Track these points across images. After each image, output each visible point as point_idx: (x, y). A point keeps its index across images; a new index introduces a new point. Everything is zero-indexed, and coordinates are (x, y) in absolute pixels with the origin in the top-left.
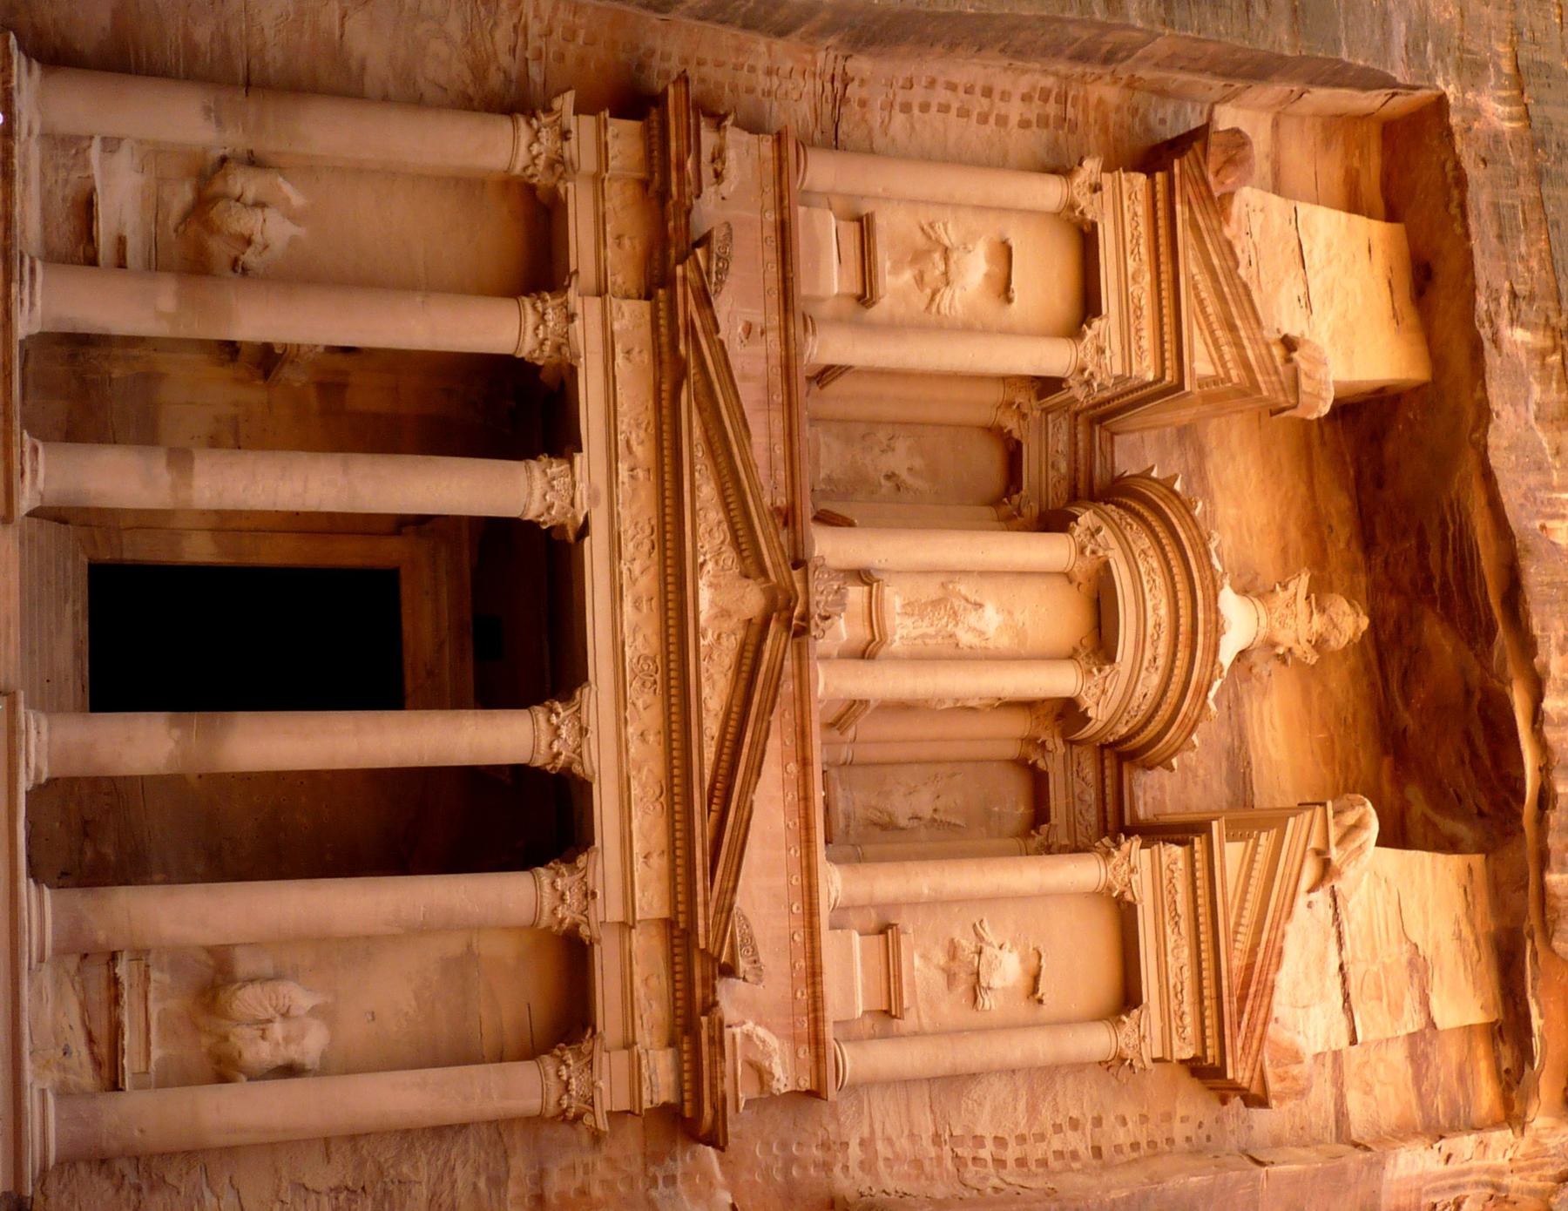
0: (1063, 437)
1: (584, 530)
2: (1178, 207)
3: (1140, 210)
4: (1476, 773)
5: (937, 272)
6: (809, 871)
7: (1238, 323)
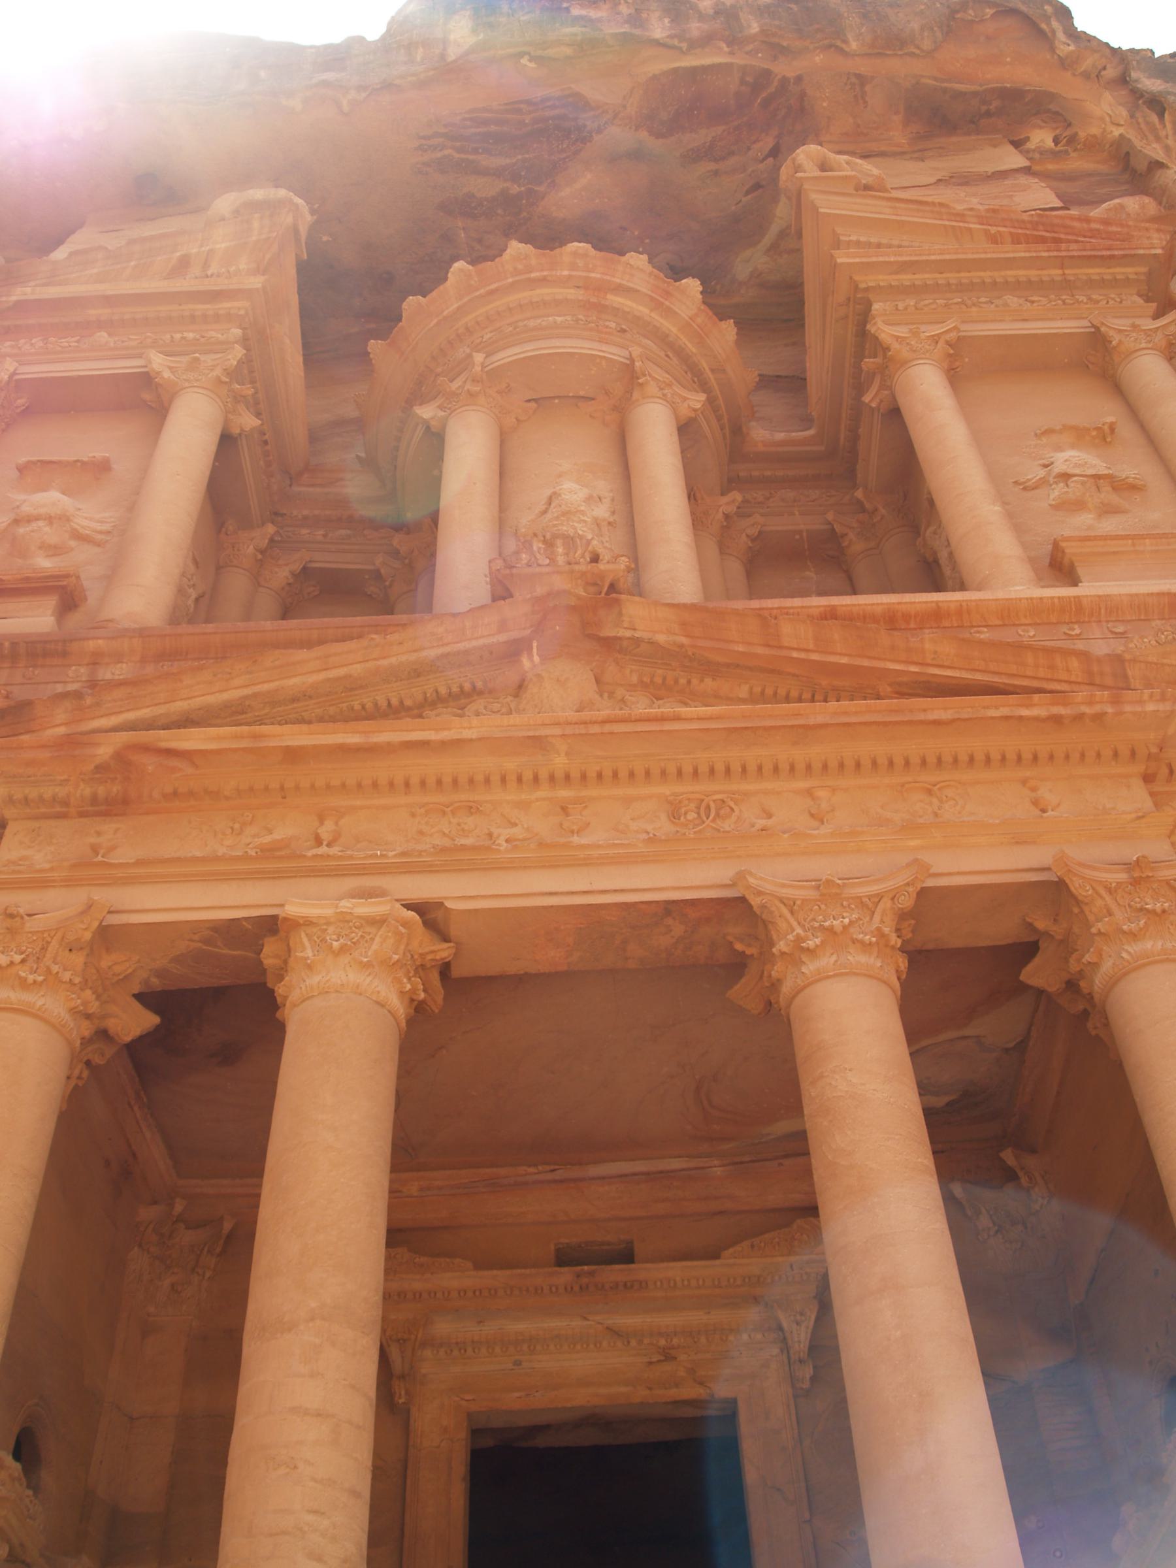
0: (304, 531)
1: (429, 914)
2: (14, 298)
3: (8, 343)
4: (732, 153)
5: (47, 529)
6: (1008, 614)
7: (178, 254)
